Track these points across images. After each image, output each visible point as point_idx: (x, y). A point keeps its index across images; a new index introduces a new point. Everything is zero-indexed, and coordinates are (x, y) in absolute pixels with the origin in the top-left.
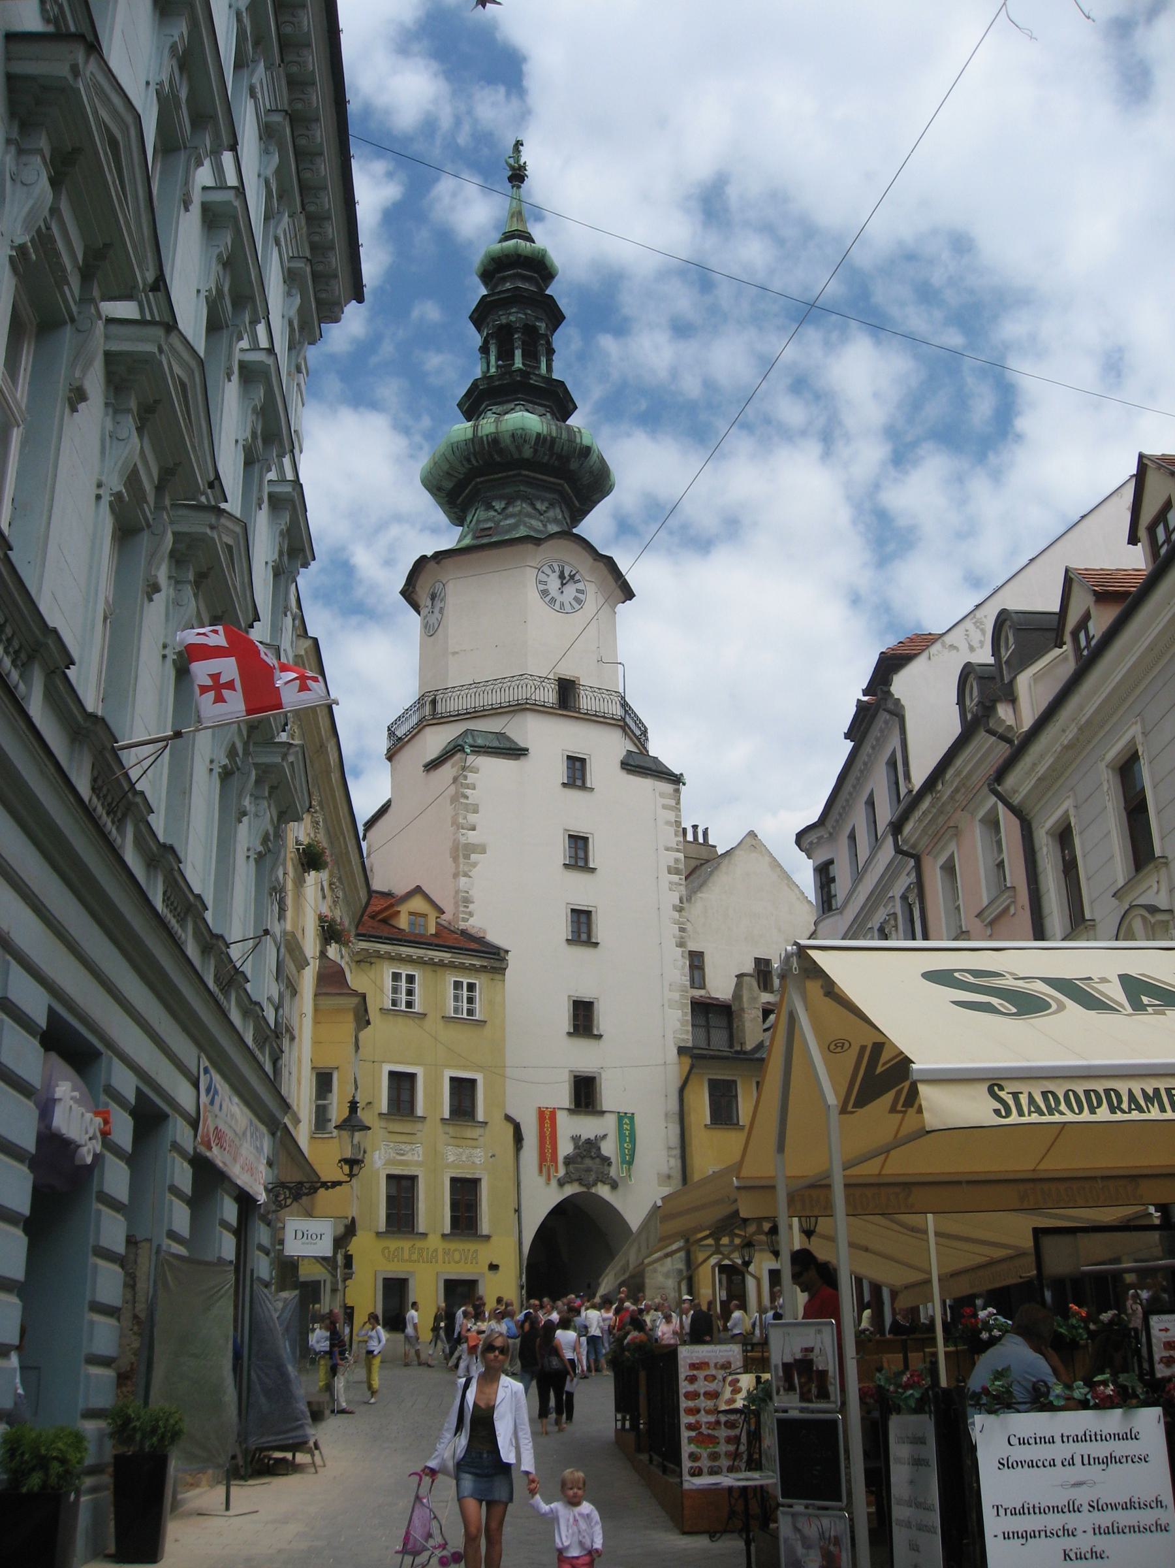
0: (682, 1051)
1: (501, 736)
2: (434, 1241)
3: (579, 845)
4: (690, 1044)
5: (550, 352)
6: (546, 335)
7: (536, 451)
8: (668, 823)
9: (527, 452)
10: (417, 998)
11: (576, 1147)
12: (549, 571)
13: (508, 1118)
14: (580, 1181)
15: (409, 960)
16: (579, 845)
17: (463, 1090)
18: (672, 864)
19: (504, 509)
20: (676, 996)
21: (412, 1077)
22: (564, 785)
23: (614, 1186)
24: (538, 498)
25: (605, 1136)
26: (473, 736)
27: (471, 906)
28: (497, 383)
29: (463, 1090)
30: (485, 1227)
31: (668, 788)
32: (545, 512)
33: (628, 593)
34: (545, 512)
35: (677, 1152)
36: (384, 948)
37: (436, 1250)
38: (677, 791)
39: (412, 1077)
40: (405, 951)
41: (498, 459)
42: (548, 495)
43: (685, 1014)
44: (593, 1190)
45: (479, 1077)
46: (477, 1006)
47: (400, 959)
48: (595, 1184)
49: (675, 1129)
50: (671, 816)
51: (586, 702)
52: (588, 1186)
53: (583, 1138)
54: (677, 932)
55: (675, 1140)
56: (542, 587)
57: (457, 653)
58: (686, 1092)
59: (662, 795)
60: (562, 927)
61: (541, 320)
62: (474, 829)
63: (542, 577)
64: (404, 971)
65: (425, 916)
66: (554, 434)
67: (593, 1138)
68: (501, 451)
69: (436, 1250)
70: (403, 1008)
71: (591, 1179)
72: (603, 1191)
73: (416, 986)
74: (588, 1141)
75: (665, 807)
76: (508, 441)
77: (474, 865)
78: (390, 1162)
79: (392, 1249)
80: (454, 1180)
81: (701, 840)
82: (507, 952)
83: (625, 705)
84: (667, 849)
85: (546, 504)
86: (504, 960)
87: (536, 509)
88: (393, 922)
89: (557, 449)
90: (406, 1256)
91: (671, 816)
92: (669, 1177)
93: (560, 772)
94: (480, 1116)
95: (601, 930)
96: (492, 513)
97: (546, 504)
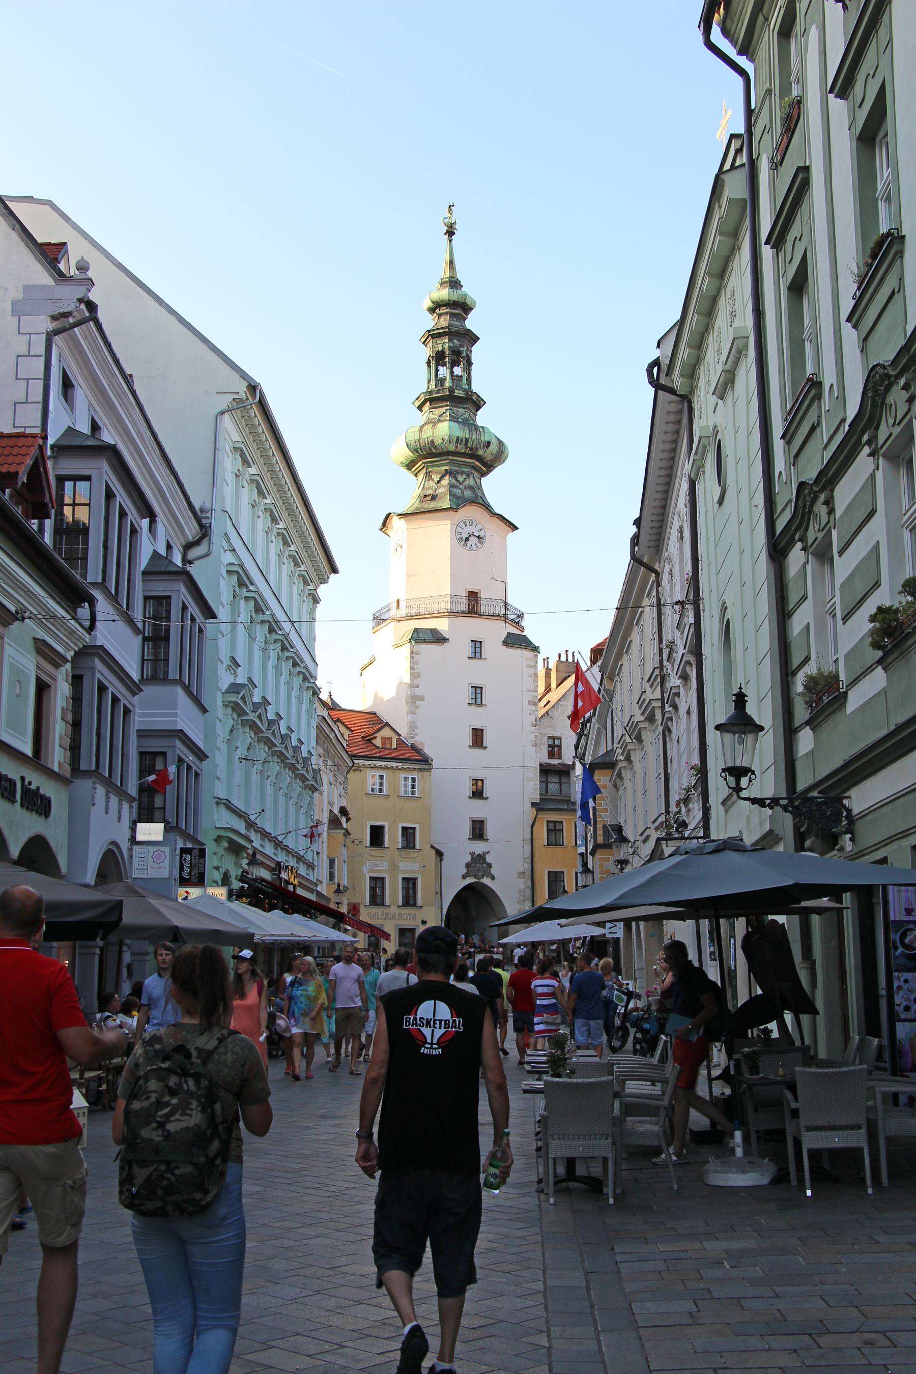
0: (533, 805)
1: (434, 631)
2: (394, 909)
3: (477, 690)
4: (538, 801)
5: (469, 364)
6: (467, 355)
7: (457, 447)
8: (530, 676)
9: (452, 448)
10: (384, 787)
11: (473, 858)
12: (462, 525)
13: (432, 847)
14: (475, 877)
15: (381, 768)
16: (477, 690)
17: (408, 834)
18: (531, 699)
19: (438, 482)
20: (531, 774)
21: (381, 828)
22: (469, 658)
23: (493, 878)
24: (459, 474)
25: (488, 852)
26: (417, 632)
27: (416, 730)
28: (435, 395)
29: (408, 834)
30: (420, 902)
31: (529, 654)
32: (463, 482)
33: (515, 528)
34: (463, 482)
35: (529, 860)
36: (367, 763)
37: (395, 914)
38: (536, 656)
39: (381, 828)
40: (378, 763)
41: (435, 451)
42: (465, 470)
43: (536, 784)
44: (481, 881)
45: (417, 826)
46: (416, 789)
47: (375, 767)
48: (482, 877)
49: (528, 847)
50: (532, 671)
51: (483, 609)
52: (479, 879)
53: (476, 854)
54: (533, 738)
55: (528, 853)
56: (458, 536)
57: (411, 575)
58: (534, 828)
59: (527, 659)
60: (468, 740)
61: (463, 346)
62: (417, 687)
63: (459, 530)
64: (378, 773)
65: (391, 739)
66: (467, 436)
67: (481, 853)
68: (435, 447)
69: (395, 914)
70: (378, 793)
71: (480, 873)
72: (486, 881)
73: (384, 781)
74: (479, 855)
75: (528, 666)
76: (440, 441)
77: (418, 707)
78: (372, 870)
79: (372, 913)
80: (403, 879)
81: (570, 660)
82: (432, 760)
83: (506, 605)
84: (529, 691)
85: (464, 476)
86: (430, 764)
87: (457, 480)
88: (373, 741)
89: (469, 444)
90: (380, 917)
91: (532, 671)
92: (524, 873)
93: (468, 650)
94: (418, 846)
95: (488, 739)
96: (431, 483)
97: (464, 476)
